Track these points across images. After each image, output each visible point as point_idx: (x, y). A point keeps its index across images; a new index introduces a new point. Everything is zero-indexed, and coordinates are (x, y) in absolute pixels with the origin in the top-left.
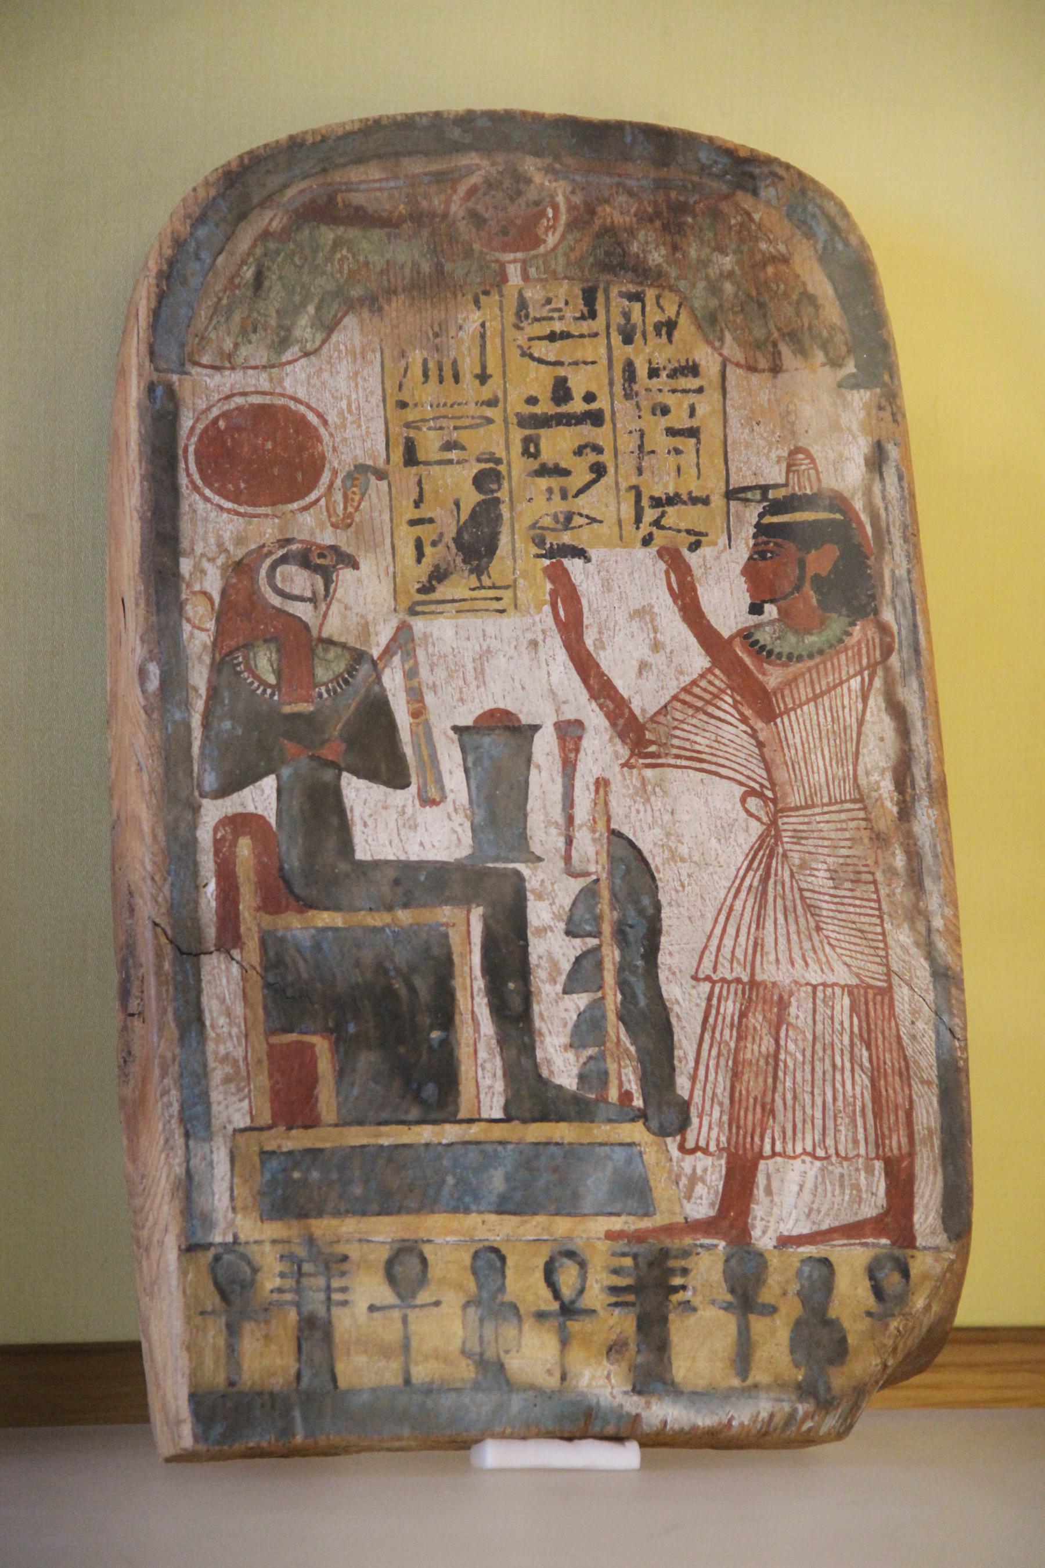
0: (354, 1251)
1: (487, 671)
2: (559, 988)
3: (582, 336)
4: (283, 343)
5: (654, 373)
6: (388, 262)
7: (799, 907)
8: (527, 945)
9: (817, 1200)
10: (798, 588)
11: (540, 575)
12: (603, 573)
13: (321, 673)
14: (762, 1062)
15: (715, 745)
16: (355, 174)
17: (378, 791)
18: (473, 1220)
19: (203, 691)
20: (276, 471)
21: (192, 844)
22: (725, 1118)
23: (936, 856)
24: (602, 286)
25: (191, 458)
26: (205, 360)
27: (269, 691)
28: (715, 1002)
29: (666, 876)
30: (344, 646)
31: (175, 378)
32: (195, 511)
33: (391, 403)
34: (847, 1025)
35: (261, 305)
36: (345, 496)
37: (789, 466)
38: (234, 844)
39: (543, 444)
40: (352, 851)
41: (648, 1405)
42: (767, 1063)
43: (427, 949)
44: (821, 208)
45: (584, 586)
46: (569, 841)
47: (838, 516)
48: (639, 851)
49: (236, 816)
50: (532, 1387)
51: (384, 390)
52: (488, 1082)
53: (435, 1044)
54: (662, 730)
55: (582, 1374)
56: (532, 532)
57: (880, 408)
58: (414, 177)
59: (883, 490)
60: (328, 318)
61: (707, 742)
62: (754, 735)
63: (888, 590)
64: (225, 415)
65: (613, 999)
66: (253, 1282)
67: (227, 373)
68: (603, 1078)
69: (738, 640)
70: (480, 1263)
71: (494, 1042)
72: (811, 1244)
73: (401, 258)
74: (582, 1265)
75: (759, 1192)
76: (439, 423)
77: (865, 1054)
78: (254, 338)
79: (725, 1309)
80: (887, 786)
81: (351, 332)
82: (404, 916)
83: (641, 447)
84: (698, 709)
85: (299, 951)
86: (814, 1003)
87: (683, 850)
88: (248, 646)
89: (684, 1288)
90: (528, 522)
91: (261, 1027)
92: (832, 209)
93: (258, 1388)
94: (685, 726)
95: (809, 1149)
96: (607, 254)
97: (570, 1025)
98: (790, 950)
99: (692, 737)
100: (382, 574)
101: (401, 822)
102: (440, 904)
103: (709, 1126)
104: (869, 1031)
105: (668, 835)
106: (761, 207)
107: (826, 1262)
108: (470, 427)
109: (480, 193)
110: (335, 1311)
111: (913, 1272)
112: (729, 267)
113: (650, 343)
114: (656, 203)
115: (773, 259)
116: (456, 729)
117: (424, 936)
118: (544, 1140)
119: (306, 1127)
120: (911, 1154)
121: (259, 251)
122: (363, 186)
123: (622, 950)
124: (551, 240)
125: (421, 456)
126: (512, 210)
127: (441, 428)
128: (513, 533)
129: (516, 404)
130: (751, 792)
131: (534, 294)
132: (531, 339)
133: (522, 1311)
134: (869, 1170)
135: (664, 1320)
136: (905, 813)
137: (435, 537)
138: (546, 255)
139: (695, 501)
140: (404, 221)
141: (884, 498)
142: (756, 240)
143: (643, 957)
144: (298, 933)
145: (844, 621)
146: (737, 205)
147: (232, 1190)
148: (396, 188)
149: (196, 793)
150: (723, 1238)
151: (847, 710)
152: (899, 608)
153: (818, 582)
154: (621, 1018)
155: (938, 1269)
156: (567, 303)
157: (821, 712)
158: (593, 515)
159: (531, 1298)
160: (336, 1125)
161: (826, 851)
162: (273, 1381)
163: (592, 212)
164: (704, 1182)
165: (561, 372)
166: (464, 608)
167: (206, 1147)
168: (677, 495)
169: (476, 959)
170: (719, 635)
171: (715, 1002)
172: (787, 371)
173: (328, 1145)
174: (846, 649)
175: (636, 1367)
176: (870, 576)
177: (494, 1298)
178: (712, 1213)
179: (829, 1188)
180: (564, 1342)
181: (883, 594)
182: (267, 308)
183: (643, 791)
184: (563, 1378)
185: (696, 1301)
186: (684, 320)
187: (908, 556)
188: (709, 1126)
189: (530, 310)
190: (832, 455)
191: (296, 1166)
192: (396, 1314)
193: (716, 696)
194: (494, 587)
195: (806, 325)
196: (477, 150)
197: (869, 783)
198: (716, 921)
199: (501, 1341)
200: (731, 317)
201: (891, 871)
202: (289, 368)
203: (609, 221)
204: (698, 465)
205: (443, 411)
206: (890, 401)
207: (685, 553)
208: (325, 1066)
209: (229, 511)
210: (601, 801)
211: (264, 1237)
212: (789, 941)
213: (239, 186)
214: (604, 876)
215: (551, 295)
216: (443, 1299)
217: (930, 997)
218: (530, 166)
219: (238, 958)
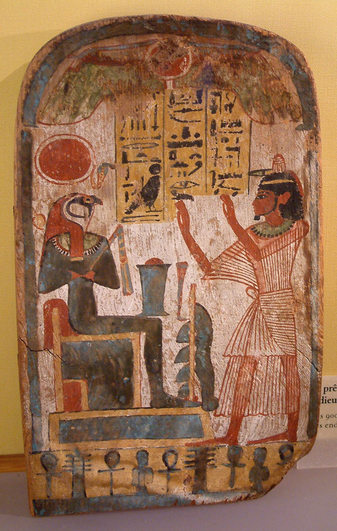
0: (93, 453)
2: (173, 361)
3: (196, 110)
4: (76, 114)
5: (223, 125)
11: (173, 206)
12: (199, 205)
13: (86, 245)
15: (237, 270)
16: (108, 43)
19: (41, 253)
21: (35, 311)
22: (232, 404)
24: (205, 89)
25: (38, 162)
27: (66, 253)
28: (231, 364)
30: (96, 235)
31: (32, 128)
33: (118, 138)
35: (67, 98)
36: (98, 176)
37: (274, 162)
38: (51, 310)
39: (177, 154)
40: (97, 313)
41: (198, 497)
44: (295, 57)
46: (180, 308)
47: (291, 181)
48: (206, 311)
51: (115, 133)
53: (125, 382)
55: (175, 489)
56: (172, 189)
57: (312, 138)
59: (310, 171)
60: (94, 104)
61: (235, 269)
62: (253, 266)
64: (51, 144)
65: (193, 364)
67: (52, 126)
68: (187, 392)
70: (139, 455)
74: (176, 455)
75: (242, 428)
78: (64, 112)
80: (301, 283)
81: (103, 109)
83: (216, 155)
85: (75, 350)
88: (58, 235)
90: (171, 185)
91: (60, 377)
92: (298, 56)
93: (57, 498)
94: (227, 264)
95: (261, 412)
97: (176, 374)
99: (229, 267)
102: (130, 332)
103: (226, 407)
106: (271, 57)
107: (265, 449)
108: (150, 147)
111: (295, 449)
112: (256, 82)
119: (76, 412)
120: (298, 411)
121: (67, 76)
123: (197, 347)
124: (185, 71)
129: (168, 138)
130: (251, 287)
132: (175, 112)
134: (282, 418)
135: (205, 471)
136: (308, 292)
147: (49, 434)
149: (37, 292)
151: (289, 255)
152: (312, 216)
153: (283, 207)
155: (304, 447)
156: (190, 97)
157: (279, 257)
163: (202, 59)
165: (187, 125)
166: (143, 219)
168: (229, 174)
169: (142, 352)
171: (231, 364)
172: (276, 124)
173: (85, 418)
174: (291, 232)
176: (302, 204)
178: (225, 436)
180: (169, 479)
183: (208, 289)
184: (168, 490)
186: (237, 104)
188: (226, 407)
191: (73, 425)
192: (108, 473)
194: (155, 211)
195: (285, 105)
196: (157, 33)
201: (301, 314)
202: (78, 124)
203: (209, 63)
206: (315, 137)
207: (231, 197)
208: (84, 390)
209: (52, 182)
210: (192, 293)
211: (60, 449)
213: (60, 47)
214: (192, 320)
215: (184, 94)
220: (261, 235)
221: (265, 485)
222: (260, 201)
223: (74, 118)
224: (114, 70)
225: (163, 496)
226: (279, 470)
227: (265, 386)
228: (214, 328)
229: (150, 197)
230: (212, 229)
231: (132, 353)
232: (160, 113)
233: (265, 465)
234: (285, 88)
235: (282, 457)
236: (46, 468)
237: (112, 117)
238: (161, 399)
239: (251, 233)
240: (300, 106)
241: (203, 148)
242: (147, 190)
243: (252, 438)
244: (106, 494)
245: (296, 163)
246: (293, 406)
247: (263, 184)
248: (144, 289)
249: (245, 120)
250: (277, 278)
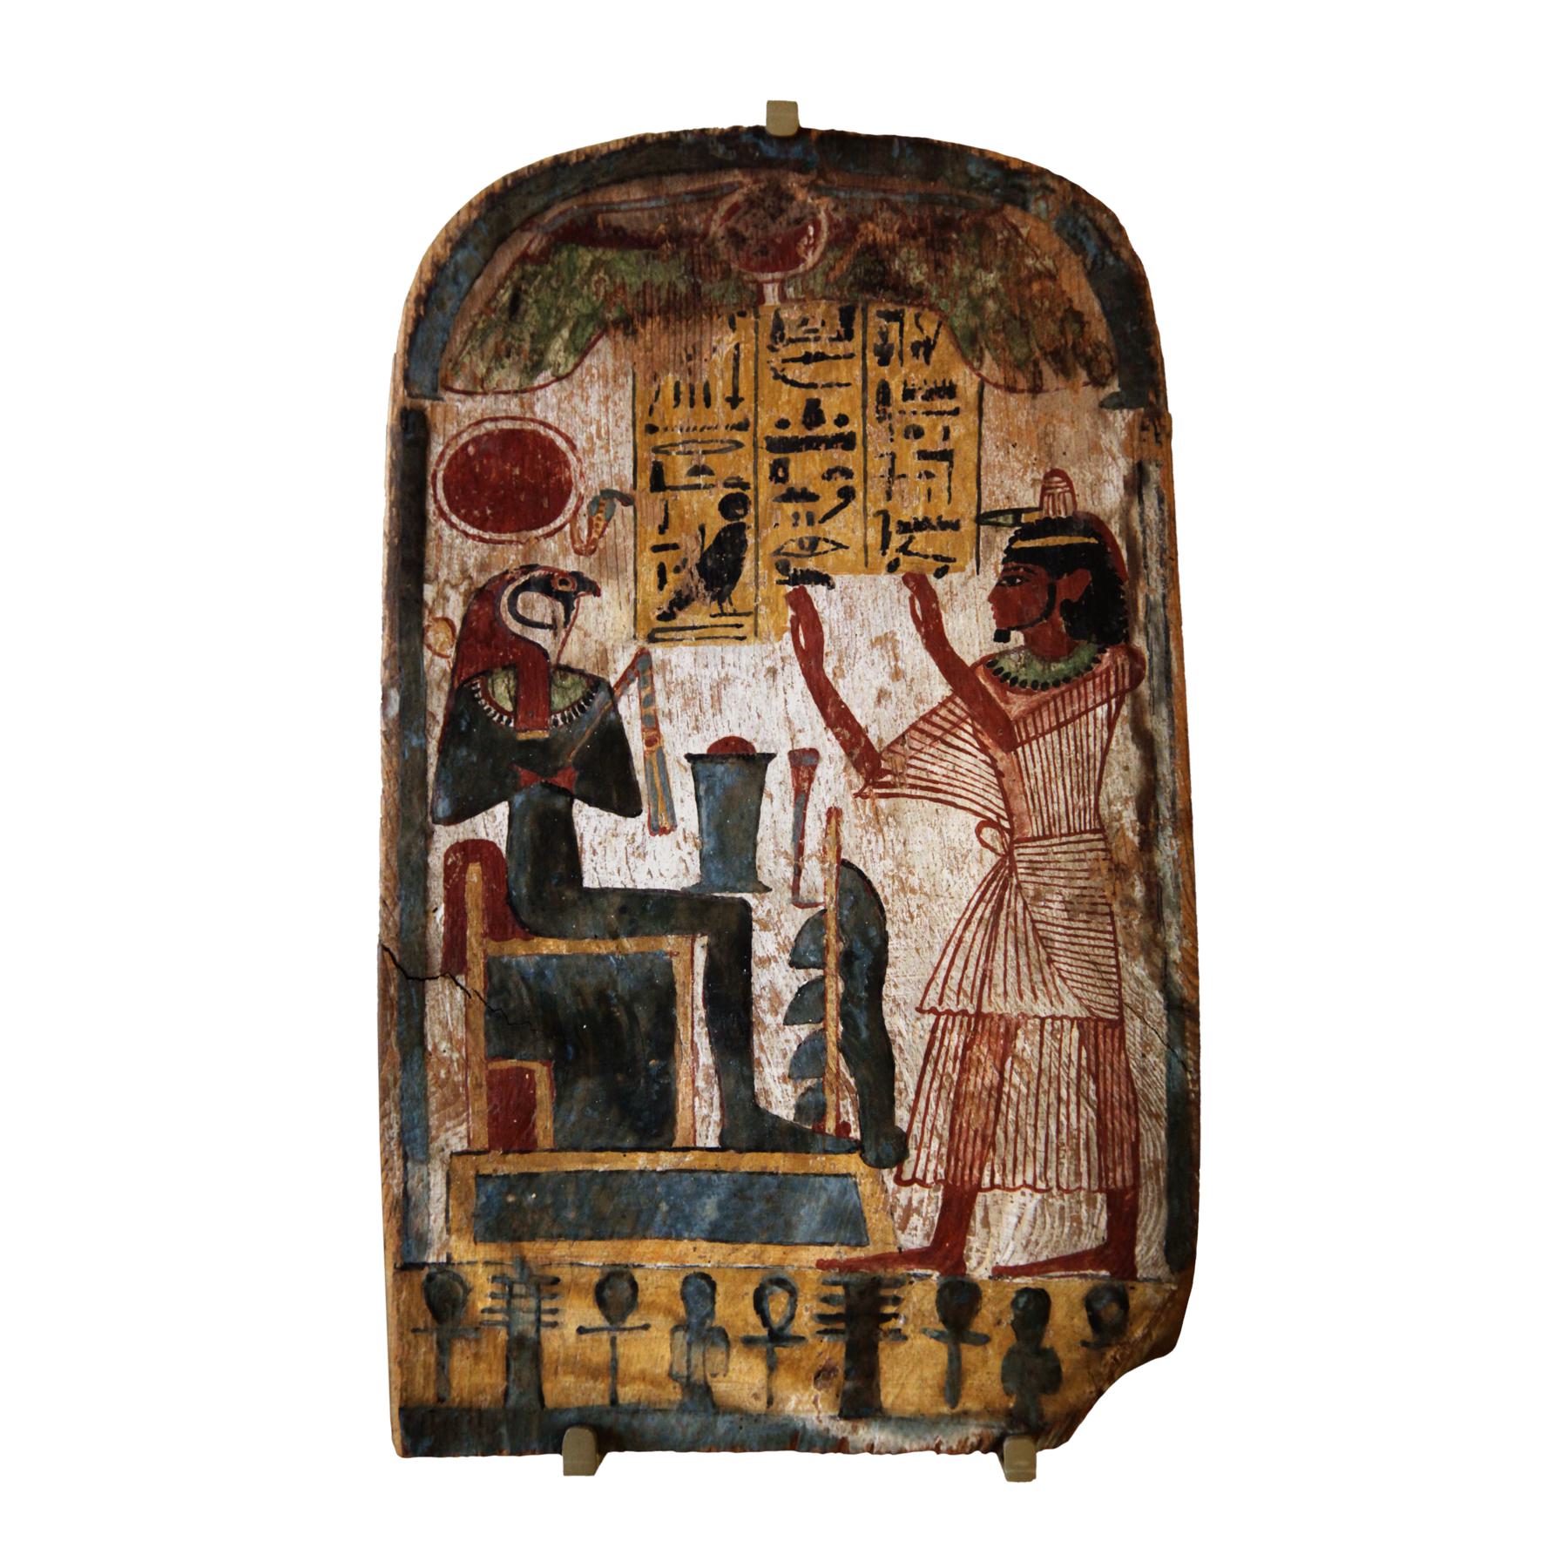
0: (565, 1274)
1: (724, 699)
2: (780, 1019)
3: (837, 357)
4: (536, 367)
5: (909, 394)
6: (645, 284)
7: (1031, 939)
8: (750, 975)
9: (1036, 1233)
10: (1047, 614)
11: (782, 602)
13: (558, 701)
14: (985, 1094)
15: (952, 775)
16: (616, 195)
17: (609, 819)
18: (684, 1246)
19: (440, 718)
20: (522, 498)
22: (944, 1150)
23: (1177, 887)
25: (440, 484)
26: (458, 385)
28: (939, 1034)
29: (895, 907)
30: (581, 673)
31: (427, 403)
32: (440, 538)
33: (640, 427)
34: (1074, 1058)
35: (515, 329)
36: (590, 522)
37: (1044, 489)
38: (464, 870)
39: (792, 468)
40: (581, 879)
41: (855, 1430)
42: (990, 1095)
43: (650, 979)
45: (827, 612)
46: (798, 872)
47: (1093, 540)
48: (869, 882)
49: (466, 842)
50: (737, 1410)
51: (634, 414)
52: (705, 1111)
53: (653, 1072)
54: (899, 759)
55: (788, 1399)
56: (776, 559)
58: (677, 195)
59: (1142, 514)
60: (581, 342)
62: (993, 764)
63: (1141, 615)
64: (475, 441)
65: (834, 1030)
66: (465, 1301)
67: (479, 398)
69: (981, 667)
70: (691, 1289)
71: (712, 1071)
72: (1027, 1275)
73: (659, 279)
74: (793, 1293)
75: (977, 1224)
76: (689, 447)
77: (1092, 1086)
78: (507, 362)
79: (937, 1338)
80: (1129, 816)
81: (604, 355)
82: (629, 944)
83: (891, 471)
84: (936, 738)
85: (523, 979)
86: (1042, 1036)
87: (914, 881)
88: (487, 673)
89: (896, 1316)
90: (772, 547)
92: (1104, 221)
93: (466, 1405)
94: (922, 756)
95: (1030, 1181)
96: (868, 272)
97: (790, 1056)
98: (1019, 983)
99: (929, 767)
100: (623, 601)
101: (630, 850)
102: (665, 934)
103: (926, 1159)
104: (1098, 1064)
105: (899, 866)
106: (1031, 221)
109: (741, 212)
110: (545, 1332)
111: (1132, 1303)
112: (992, 284)
113: (907, 364)
114: (921, 219)
115: (1039, 275)
116: (689, 757)
117: (648, 965)
118: (758, 1169)
119: (522, 1152)
120: (1136, 1187)
121: (516, 275)
122: (623, 207)
123: (846, 982)
124: (811, 259)
125: (669, 481)
126: (773, 229)
127: (690, 453)
128: (757, 560)
130: (988, 823)
131: (790, 315)
132: (785, 361)
133: (730, 1336)
134: (1091, 1203)
136: (1148, 841)
137: (679, 563)
138: (806, 272)
139: (944, 525)
140: (663, 242)
141: (1142, 521)
142: (1023, 255)
143: (867, 989)
144: (522, 959)
145: (1094, 647)
146: (1005, 221)
147: (447, 1211)
148: (659, 208)
150: (937, 1269)
153: (1068, 609)
154: (841, 1049)
155: (1159, 1299)
156: (823, 324)
157: (1064, 741)
158: (839, 540)
159: (740, 1324)
160: (552, 1151)
161: (1062, 882)
162: (481, 1398)
164: (919, 1214)
165: (814, 394)
166: (704, 635)
167: (424, 1169)
168: (926, 519)
169: (699, 988)
170: (962, 662)
171: (939, 1034)
173: (544, 1170)
174: (1094, 676)
175: (844, 1393)
176: (1123, 602)
177: (702, 1323)
178: (927, 1244)
179: (1048, 1220)
180: (772, 1368)
181: (1136, 620)
182: (521, 332)
184: (770, 1402)
185: (908, 1331)
186: (943, 340)
187: (1164, 581)
188: (926, 1159)
189: (786, 331)
190: (1090, 478)
192: (605, 1336)
193: (955, 725)
194: (735, 614)
196: (740, 167)
197: (1110, 813)
198: (944, 952)
199: (708, 1365)
200: (992, 335)
201: (1129, 902)
202: (540, 393)
204: (949, 489)
205: (692, 435)
206: (1155, 424)
207: (932, 579)
208: (543, 1091)
209: (474, 537)
212: (1018, 973)
213: (504, 210)
216: (652, 1323)
217: (1164, 1030)
218: (793, 182)
219: (463, 983)
220: (1014, 680)
221: (1052, 1407)
222: (1010, 590)
223: (532, 378)
224: (633, 259)
225: (756, 1418)
226: (1087, 1363)
227: (1037, 1104)
228: (891, 929)
229: (720, 577)
232: (746, 367)
233: (1046, 1343)
234: (1070, 300)
235: (1095, 1320)
237: (626, 375)
239: (988, 678)
240: (1111, 345)
241: (857, 452)
242: (715, 561)
243: (1006, 1258)
244: (599, 1402)
245: (1105, 493)
246: (1119, 1170)
247: (1015, 546)
248: (704, 819)
249: (965, 380)
250: (1061, 798)
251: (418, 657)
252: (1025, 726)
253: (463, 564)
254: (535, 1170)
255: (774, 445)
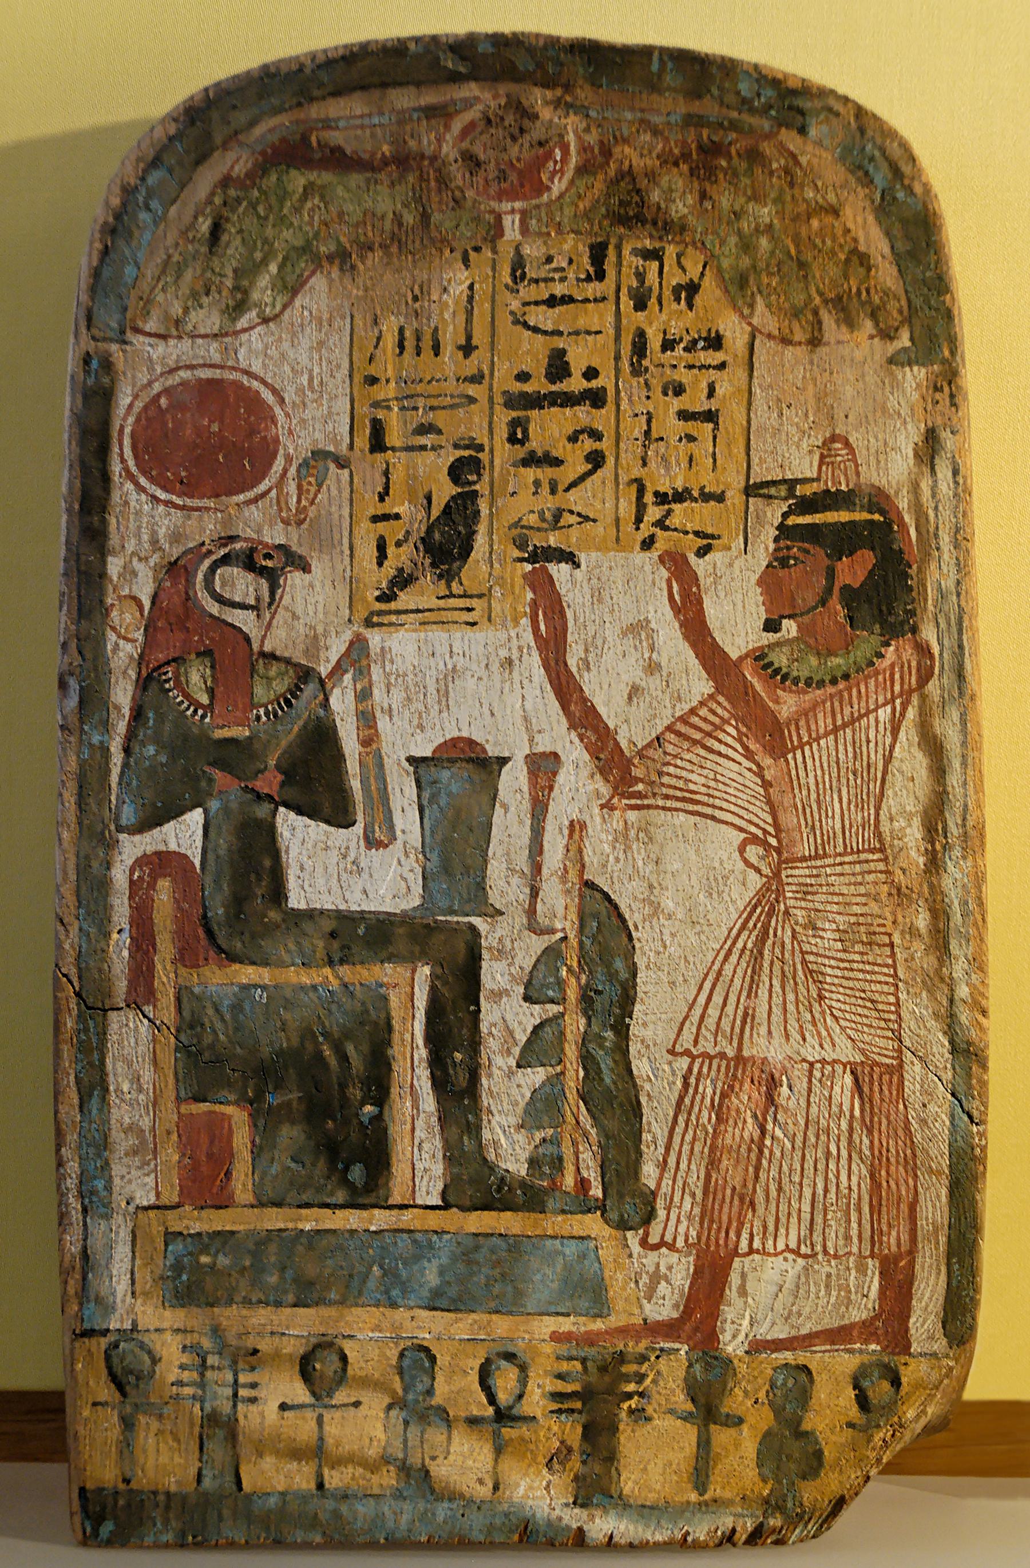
0: (265, 1345)
3: (586, 300)
4: (240, 307)
5: (668, 345)
7: (800, 973)
11: (519, 581)
12: (595, 581)
13: (260, 692)
14: (743, 1150)
15: (712, 784)
16: (336, 108)
17: (316, 830)
18: (401, 1315)
19: (126, 711)
21: (103, 885)
22: (697, 1211)
24: (613, 241)
25: (127, 442)
27: (200, 712)
30: (288, 661)
31: (114, 347)
32: (126, 503)
33: (358, 378)
34: (846, 1108)
35: (216, 263)
36: (299, 487)
37: (822, 457)
38: (152, 886)
41: (592, 1518)
44: (883, 151)
46: (535, 893)
47: (877, 517)
48: (616, 907)
53: (365, 1120)
55: (518, 1485)
57: (937, 389)
60: (291, 279)
61: (703, 780)
62: (760, 774)
64: (166, 391)
65: (574, 1074)
68: (558, 1163)
70: (406, 1362)
74: (523, 1368)
75: (732, 1294)
77: (866, 1141)
78: (205, 300)
79: (685, 1419)
80: (914, 834)
81: (319, 292)
83: (647, 433)
85: (217, 1010)
86: (810, 1082)
91: (170, 1093)
92: (894, 149)
94: (679, 762)
95: (793, 1245)
97: (522, 1104)
99: (684, 774)
103: (678, 1219)
106: (809, 148)
107: (805, 1369)
108: (452, 407)
111: (904, 1380)
112: (767, 220)
114: (684, 142)
120: (912, 1252)
121: (218, 200)
124: (557, 187)
129: (504, 380)
130: (754, 840)
134: (862, 1269)
135: (613, 1429)
136: (934, 863)
141: (934, 495)
145: (875, 640)
147: (132, 1273)
149: (113, 827)
151: (872, 745)
152: (943, 625)
157: (841, 748)
161: (835, 908)
163: (607, 153)
165: (560, 343)
166: (427, 618)
171: (692, 1081)
172: (828, 344)
173: (241, 1228)
174: (877, 673)
176: (910, 589)
178: (675, 1315)
180: (498, 1451)
183: (622, 838)
184: (496, 1488)
186: (709, 284)
188: (678, 1219)
191: (205, 1250)
192: (310, 1415)
193: (717, 727)
194: (465, 596)
195: (854, 290)
196: (476, 79)
201: (913, 932)
202: (244, 337)
203: (627, 163)
206: (947, 384)
207: (692, 558)
208: (242, 1138)
209: (167, 503)
210: (573, 848)
211: (166, 1325)
213: (203, 121)
214: (572, 935)
215: (552, 252)
221: (813, 1494)
222: (781, 573)
223: (234, 320)
224: (353, 184)
228: (640, 960)
230: (637, 660)
231: (390, 1028)
234: (855, 240)
235: (863, 1402)
236: (120, 1387)
238: (476, 1185)
239: (755, 672)
242: (442, 534)
243: (765, 1332)
245: (889, 465)
246: (894, 1233)
248: (427, 833)
249: (733, 330)
251: (100, 641)
252: (798, 729)
253: (154, 534)
254: (234, 1228)
255: (511, 401)
